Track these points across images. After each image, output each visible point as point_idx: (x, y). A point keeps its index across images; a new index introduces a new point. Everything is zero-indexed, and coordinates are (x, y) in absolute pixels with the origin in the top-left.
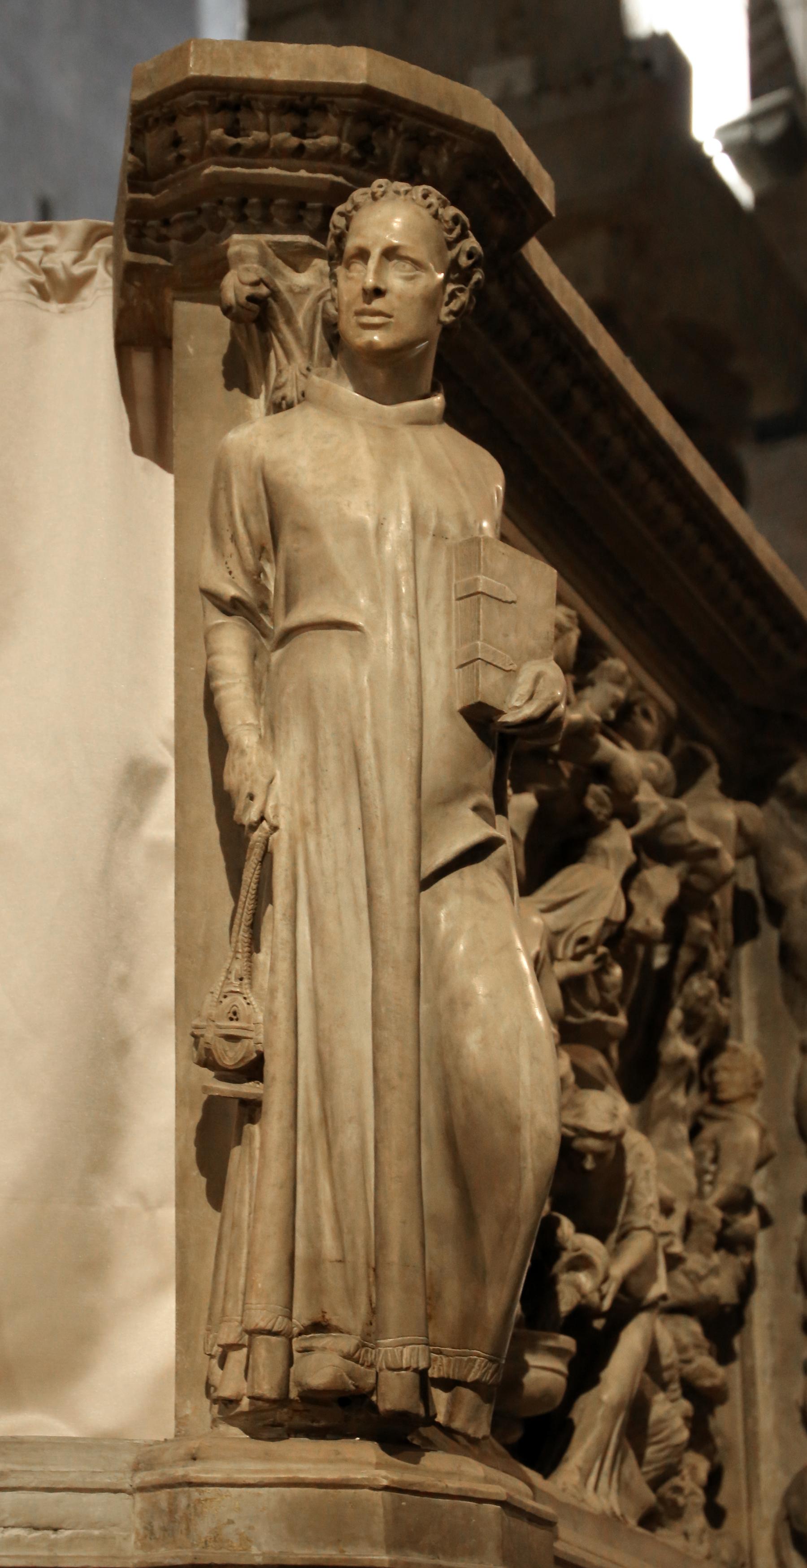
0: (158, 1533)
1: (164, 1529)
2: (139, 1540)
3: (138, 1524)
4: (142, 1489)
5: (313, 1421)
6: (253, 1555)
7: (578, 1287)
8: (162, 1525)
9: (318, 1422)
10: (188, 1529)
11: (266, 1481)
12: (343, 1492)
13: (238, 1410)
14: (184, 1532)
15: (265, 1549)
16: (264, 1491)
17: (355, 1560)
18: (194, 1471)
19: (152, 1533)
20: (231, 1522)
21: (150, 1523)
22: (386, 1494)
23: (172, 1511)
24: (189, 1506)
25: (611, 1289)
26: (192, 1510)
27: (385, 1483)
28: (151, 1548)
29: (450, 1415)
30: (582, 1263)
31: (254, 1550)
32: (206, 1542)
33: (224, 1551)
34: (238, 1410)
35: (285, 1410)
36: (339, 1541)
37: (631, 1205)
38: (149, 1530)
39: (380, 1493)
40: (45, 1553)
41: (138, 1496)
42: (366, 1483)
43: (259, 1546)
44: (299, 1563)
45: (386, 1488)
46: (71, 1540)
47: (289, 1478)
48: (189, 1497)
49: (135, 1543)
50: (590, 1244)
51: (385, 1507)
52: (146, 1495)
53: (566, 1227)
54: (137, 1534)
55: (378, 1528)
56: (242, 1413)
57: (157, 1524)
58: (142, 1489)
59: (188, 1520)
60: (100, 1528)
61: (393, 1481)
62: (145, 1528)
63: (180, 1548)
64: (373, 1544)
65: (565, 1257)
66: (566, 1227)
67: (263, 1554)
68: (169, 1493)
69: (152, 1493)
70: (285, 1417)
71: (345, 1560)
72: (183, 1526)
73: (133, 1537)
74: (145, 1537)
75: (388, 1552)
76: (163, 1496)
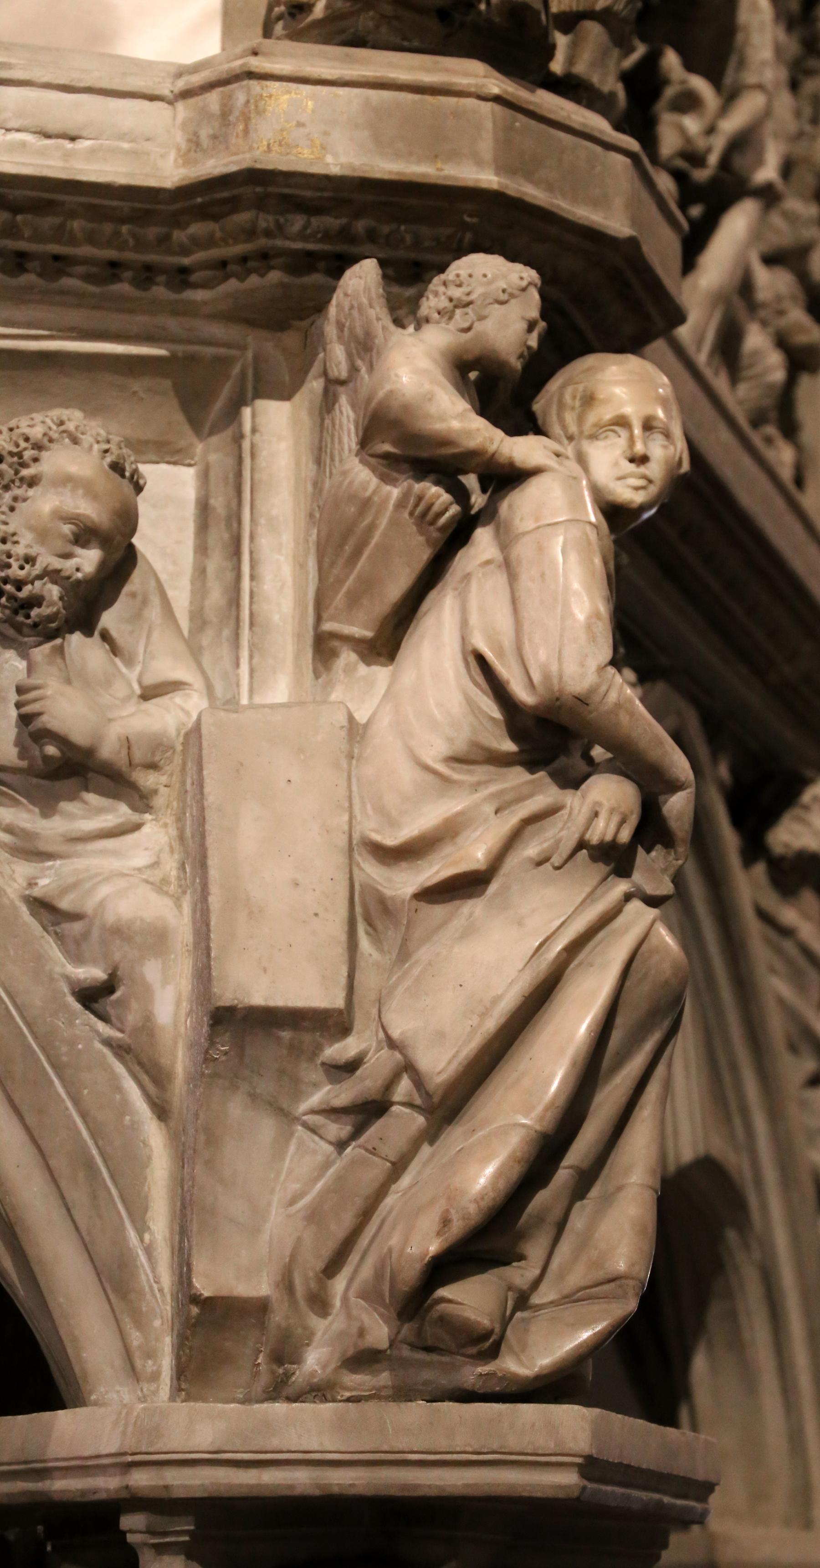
0: (205, 141)
1: (214, 137)
2: (181, 156)
3: (180, 138)
4: (186, 94)
5: (403, 39)
6: (328, 164)
7: (682, 130)
8: (211, 132)
9: (410, 41)
10: (246, 131)
11: (347, 78)
12: (442, 99)
13: (311, 18)
14: (241, 134)
15: (343, 159)
16: (342, 92)
17: (456, 179)
18: (256, 64)
19: (198, 144)
20: (300, 125)
21: (196, 134)
22: (498, 108)
23: (225, 113)
24: (248, 102)
25: (718, 145)
26: (253, 107)
27: (496, 90)
28: (196, 162)
29: (571, 60)
30: (688, 102)
31: (329, 159)
32: (269, 145)
33: (293, 158)
34: (311, 18)
35: (371, 13)
36: (436, 157)
37: (742, 64)
38: (195, 142)
39: (490, 104)
40: (60, 164)
41: (180, 106)
42: (473, 89)
43: (335, 155)
44: (386, 177)
45: (497, 99)
46: (92, 151)
47: (377, 77)
48: (249, 91)
49: (176, 160)
50: (699, 84)
51: (494, 122)
52: (192, 101)
53: (671, 60)
54: (179, 149)
55: (486, 145)
56: (317, 24)
57: (204, 134)
58: (186, 94)
59: (247, 120)
60: (132, 141)
61: (506, 92)
62: (189, 141)
63: (235, 154)
64: (479, 163)
65: (669, 92)
66: (671, 60)
67: (342, 165)
68: (222, 92)
69: (200, 97)
70: (371, 24)
71: (445, 177)
72: (241, 127)
73: (172, 156)
74: (189, 151)
75: (497, 174)
76: (213, 99)
